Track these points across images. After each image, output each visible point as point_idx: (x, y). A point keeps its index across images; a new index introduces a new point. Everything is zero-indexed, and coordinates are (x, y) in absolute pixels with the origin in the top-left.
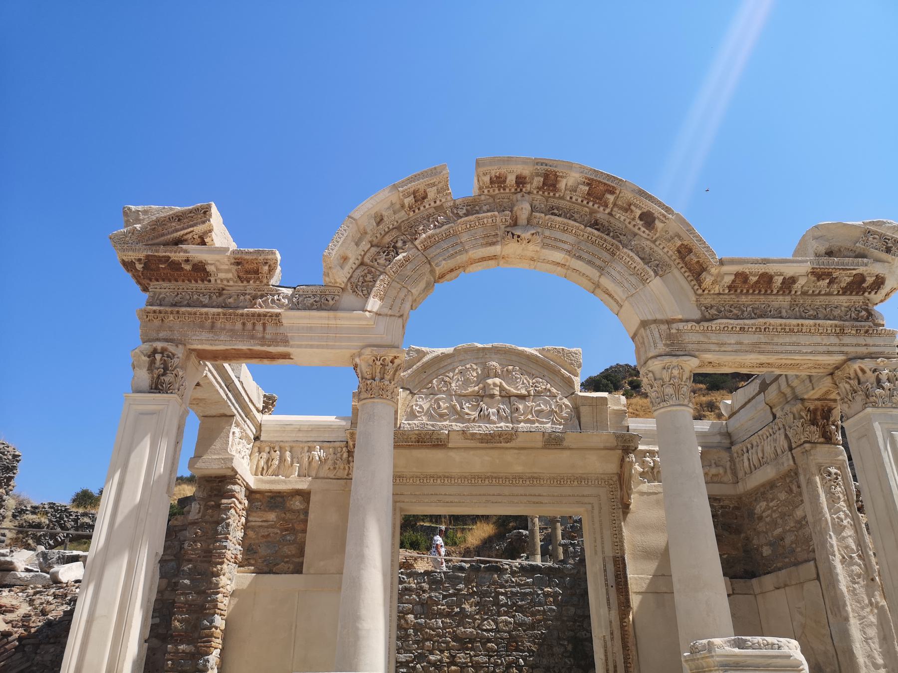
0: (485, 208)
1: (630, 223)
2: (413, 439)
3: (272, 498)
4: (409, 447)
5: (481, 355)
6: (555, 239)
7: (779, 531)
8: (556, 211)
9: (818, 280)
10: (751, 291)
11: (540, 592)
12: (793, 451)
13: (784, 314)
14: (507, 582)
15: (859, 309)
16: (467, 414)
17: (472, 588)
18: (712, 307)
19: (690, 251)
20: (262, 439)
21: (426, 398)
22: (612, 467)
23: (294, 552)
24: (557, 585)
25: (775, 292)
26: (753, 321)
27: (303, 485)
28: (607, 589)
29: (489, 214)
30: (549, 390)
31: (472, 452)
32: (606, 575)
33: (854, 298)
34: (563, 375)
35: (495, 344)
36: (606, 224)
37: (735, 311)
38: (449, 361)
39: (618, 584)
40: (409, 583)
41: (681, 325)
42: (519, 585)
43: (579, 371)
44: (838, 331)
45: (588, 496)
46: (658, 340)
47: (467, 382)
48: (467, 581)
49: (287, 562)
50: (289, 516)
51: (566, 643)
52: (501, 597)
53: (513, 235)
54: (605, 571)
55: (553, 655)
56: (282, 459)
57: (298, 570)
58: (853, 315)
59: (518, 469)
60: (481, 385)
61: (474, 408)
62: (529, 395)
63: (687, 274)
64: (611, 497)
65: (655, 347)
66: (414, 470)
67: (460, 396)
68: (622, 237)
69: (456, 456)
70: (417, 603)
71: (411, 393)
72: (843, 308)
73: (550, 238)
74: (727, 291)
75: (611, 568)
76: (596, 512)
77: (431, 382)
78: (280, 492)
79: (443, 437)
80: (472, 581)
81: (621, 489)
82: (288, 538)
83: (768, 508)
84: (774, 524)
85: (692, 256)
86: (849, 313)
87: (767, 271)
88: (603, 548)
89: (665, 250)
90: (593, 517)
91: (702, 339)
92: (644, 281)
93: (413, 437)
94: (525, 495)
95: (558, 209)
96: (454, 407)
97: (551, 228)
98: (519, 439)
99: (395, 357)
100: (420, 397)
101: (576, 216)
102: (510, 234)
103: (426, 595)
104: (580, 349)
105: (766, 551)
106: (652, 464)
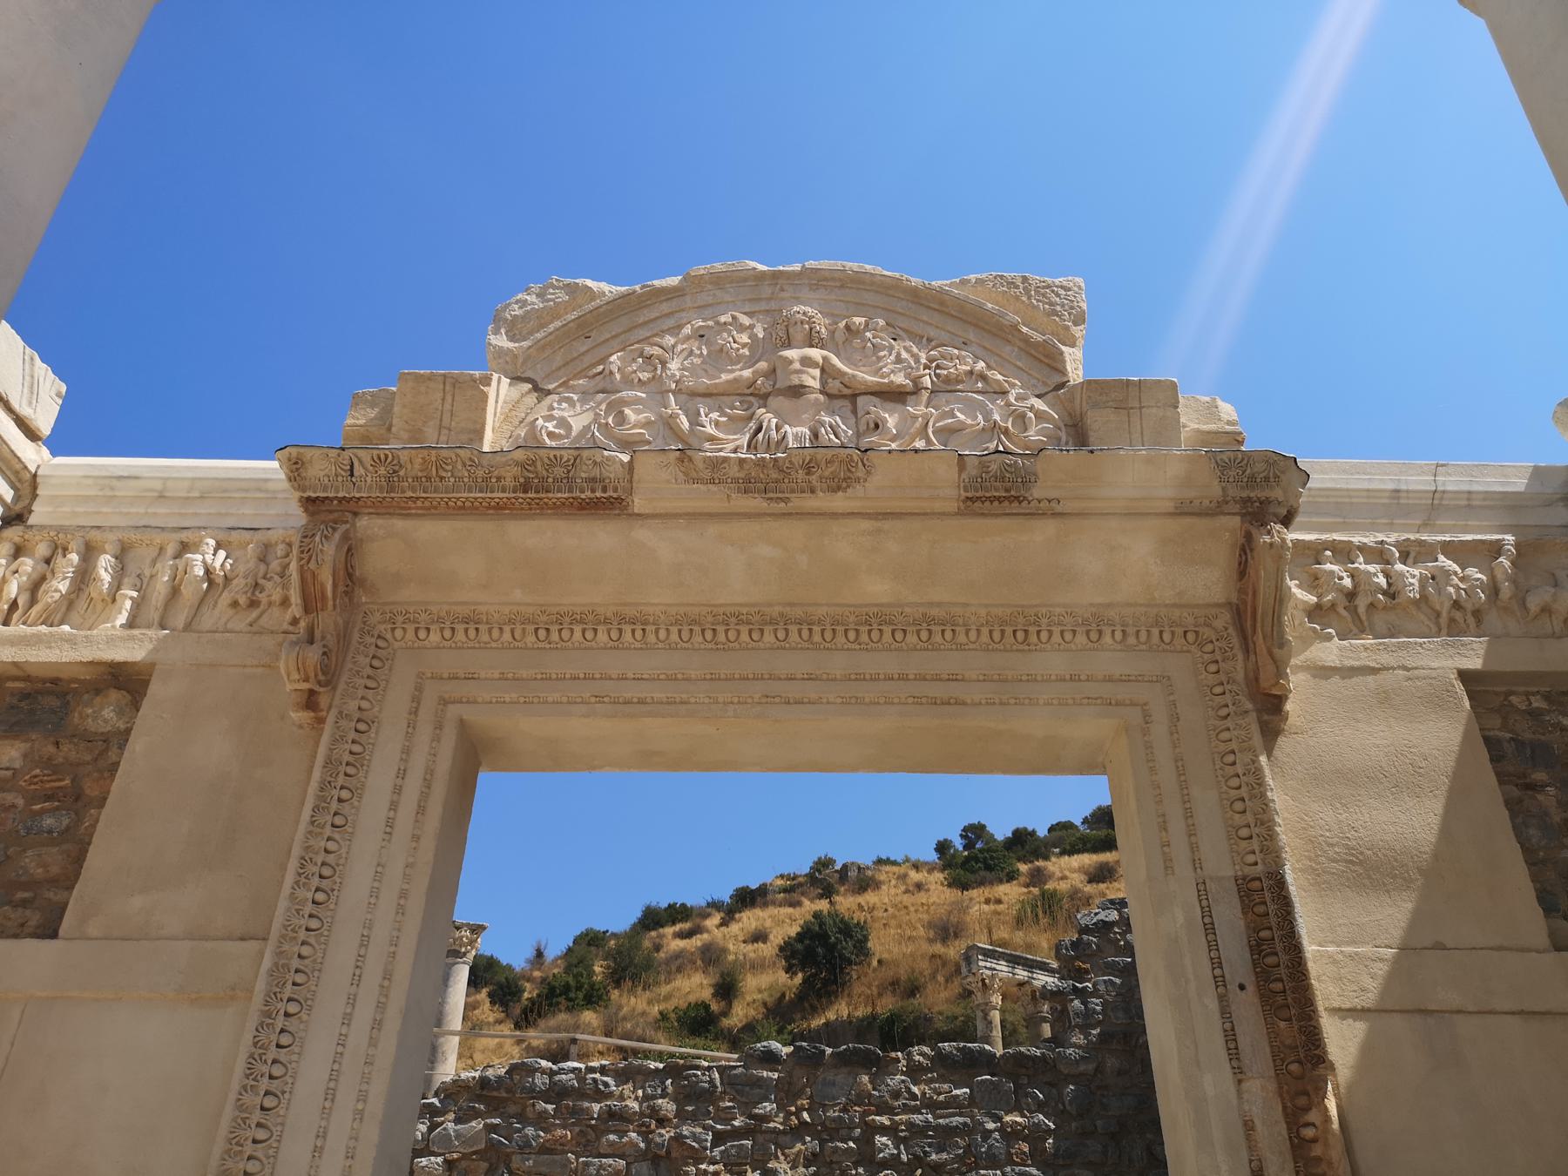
2: (509, 482)
3: (25, 696)
4: (499, 509)
5: (767, 291)
11: (991, 1126)
14: (896, 1095)
16: (712, 439)
17: (798, 1114)
20: (32, 520)
21: (583, 401)
22: (1208, 583)
23: (55, 870)
24: (1041, 1107)
27: (133, 651)
28: (1222, 998)
30: (983, 377)
31: (713, 529)
32: (1213, 946)
34: (1026, 339)
35: (811, 264)
38: (665, 308)
39: (1264, 975)
40: (622, 1098)
42: (931, 1105)
43: (1078, 331)
47: (720, 357)
48: (786, 1094)
49: (24, 903)
50: (69, 751)
52: (881, 1140)
54: (1210, 929)
56: (84, 576)
57: (49, 931)
59: (877, 590)
60: (763, 365)
61: (736, 424)
62: (917, 389)
64: (1211, 679)
66: (518, 595)
67: (694, 394)
69: (661, 544)
70: (643, 1156)
71: (536, 388)
76: (1160, 729)
77: (604, 360)
78: (55, 681)
79: (612, 473)
80: (799, 1094)
81: (1247, 648)
82: (49, 821)
88: (1194, 848)
90: (1149, 746)
93: (510, 474)
94: (903, 678)
96: (669, 424)
98: (876, 480)
100: (568, 400)
103: (667, 1134)
104: (1080, 280)
106: (1347, 582)
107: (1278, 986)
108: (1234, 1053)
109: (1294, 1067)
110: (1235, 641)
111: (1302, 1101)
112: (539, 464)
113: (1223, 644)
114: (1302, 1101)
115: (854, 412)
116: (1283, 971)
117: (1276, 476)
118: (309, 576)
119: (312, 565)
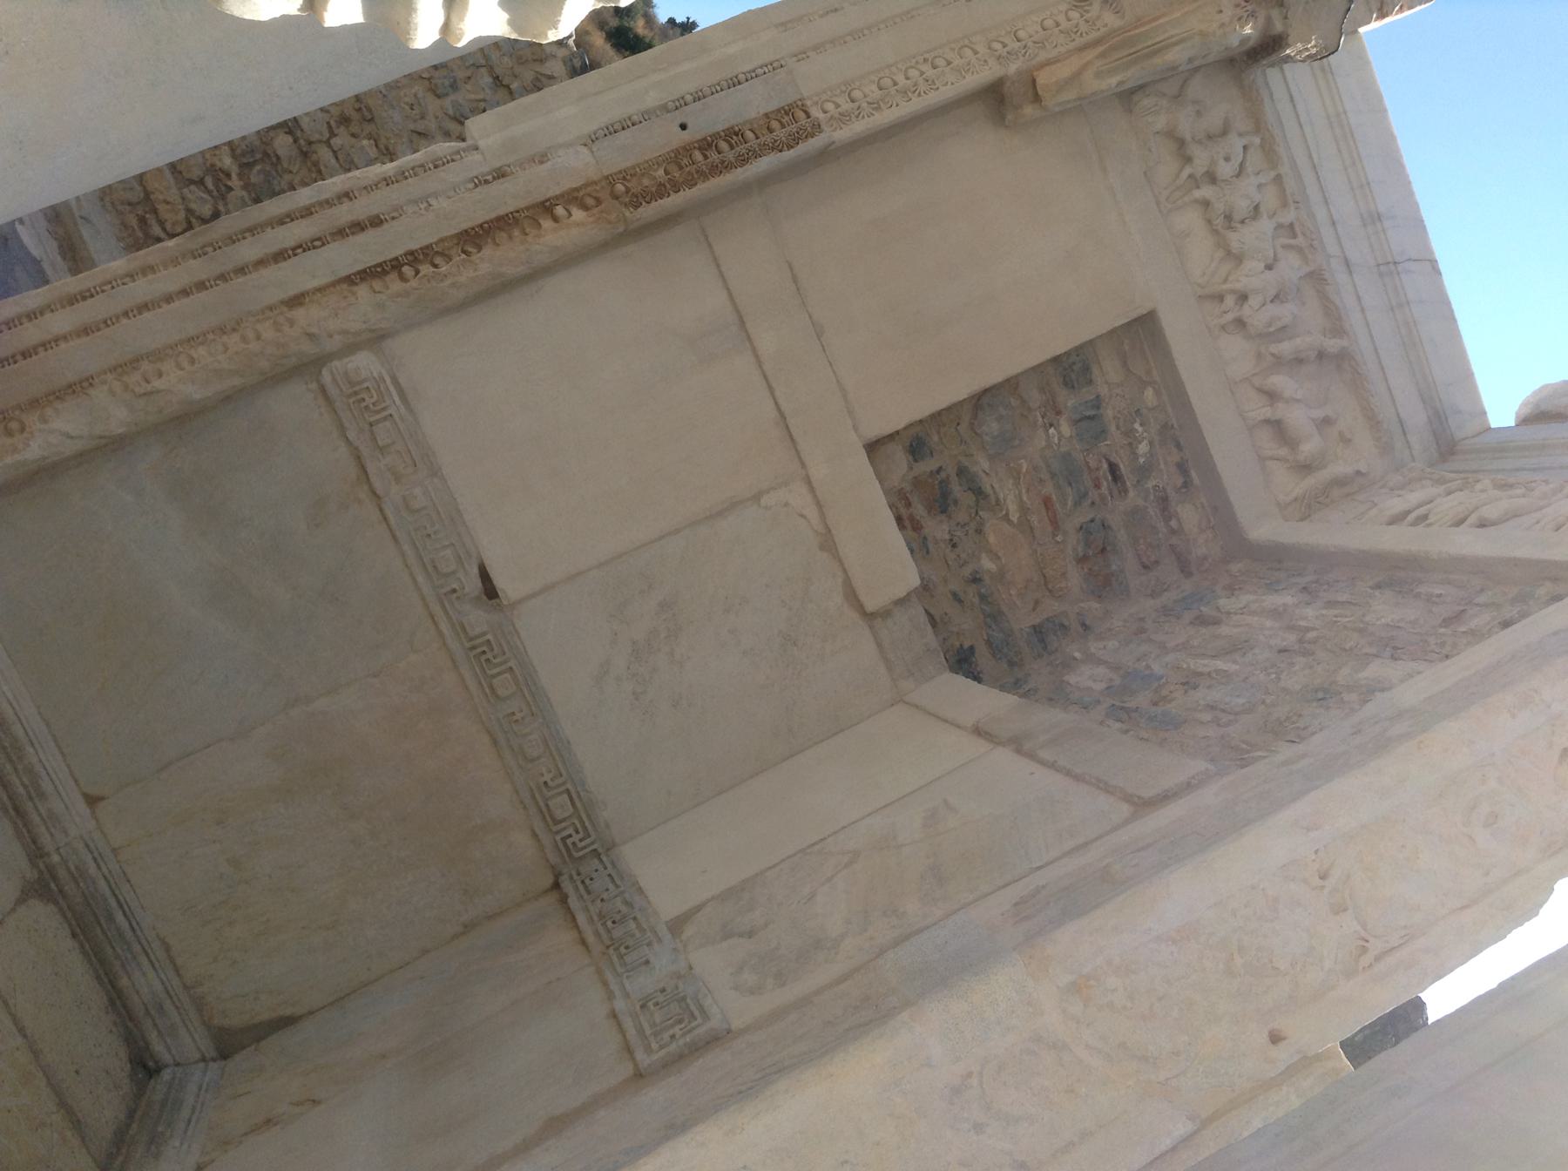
32: (716, 89)
39: (706, 145)
54: (735, 82)
75: (752, 103)
108: (611, 130)
109: (620, 187)
111: (590, 201)
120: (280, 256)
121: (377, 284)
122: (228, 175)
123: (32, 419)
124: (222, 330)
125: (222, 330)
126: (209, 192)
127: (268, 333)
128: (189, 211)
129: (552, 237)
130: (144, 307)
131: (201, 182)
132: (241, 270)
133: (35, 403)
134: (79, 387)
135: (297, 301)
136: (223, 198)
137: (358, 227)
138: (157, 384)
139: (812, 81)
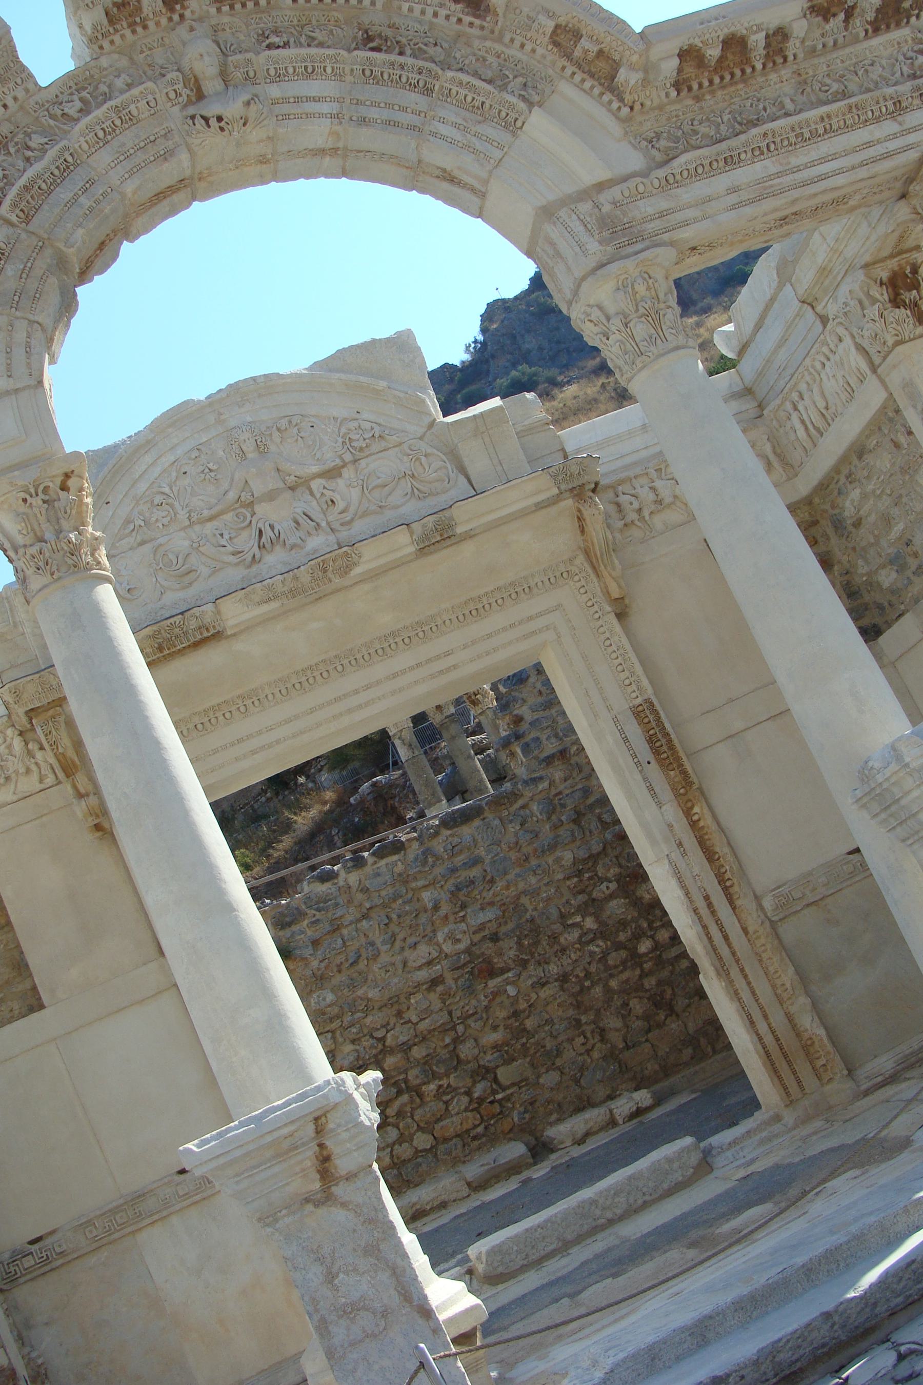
0: (119, 83)
1: (435, 15)
6: (298, 100)
7: (899, 528)
8: (274, 39)
9: (826, 20)
10: (717, 80)
12: (879, 370)
13: (789, 106)
15: (911, 54)
18: (658, 136)
19: (577, 35)
25: (759, 66)
26: (742, 137)
29: (135, 91)
32: (630, 748)
33: (896, 35)
36: (389, 33)
37: (703, 129)
39: (656, 752)
41: (615, 192)
44: (891, 108)
45: (540, 615)
46: (584, 238)
51: (578, 919)
53: (206, 120)
54: (626, 740)
55: (563, 950)
58: (905, 69)
63: (587, 85)
65: (585, 253)
68: (431, 51)
72: (884, 62)
73: (285, 100)
74: (674, 93)
75: (635, 731)
83: (864, 496)
84: (887, 520)
85: (585, 43)
86: (897, 68)
87: (733, 29)
89: (528, 47)
91: (664, 205)
92: (513, 126)
95: (276, 32)
97: (279, 78)
98: (363, 559)
99: (67, 476)
101: (319, 35)
102: (199, 121)
105: (887, 577)
107: (665, 755)
108: (654, 795)
109: (682, 791)
110: (590, 570)
111: (689, 804)
112: (162, 631)
113: (584, 574)
114: (689, 804)
115: (312, 494)
116: (665, 748)
117: (583, 470)
118: (61, 757)
119: (61, 750)
120: (726, 938)
121: (735, 897)
122: (440, 1086)
123: (806, 1035)
124: (760, 961)
125: (760, 961)
126: (453, 1098)
127: (763, 941)
128: (466, 1110)
129: (707, 821)
130: (753, 993)
131: (447, 1103)
132: (734, 954)
133: (798, 1035)
134: (790, 1017)
135: (745, 930)
136: (455, 1089)
137: (710, 905)
138: (788, 985)
139: (621, 704)
